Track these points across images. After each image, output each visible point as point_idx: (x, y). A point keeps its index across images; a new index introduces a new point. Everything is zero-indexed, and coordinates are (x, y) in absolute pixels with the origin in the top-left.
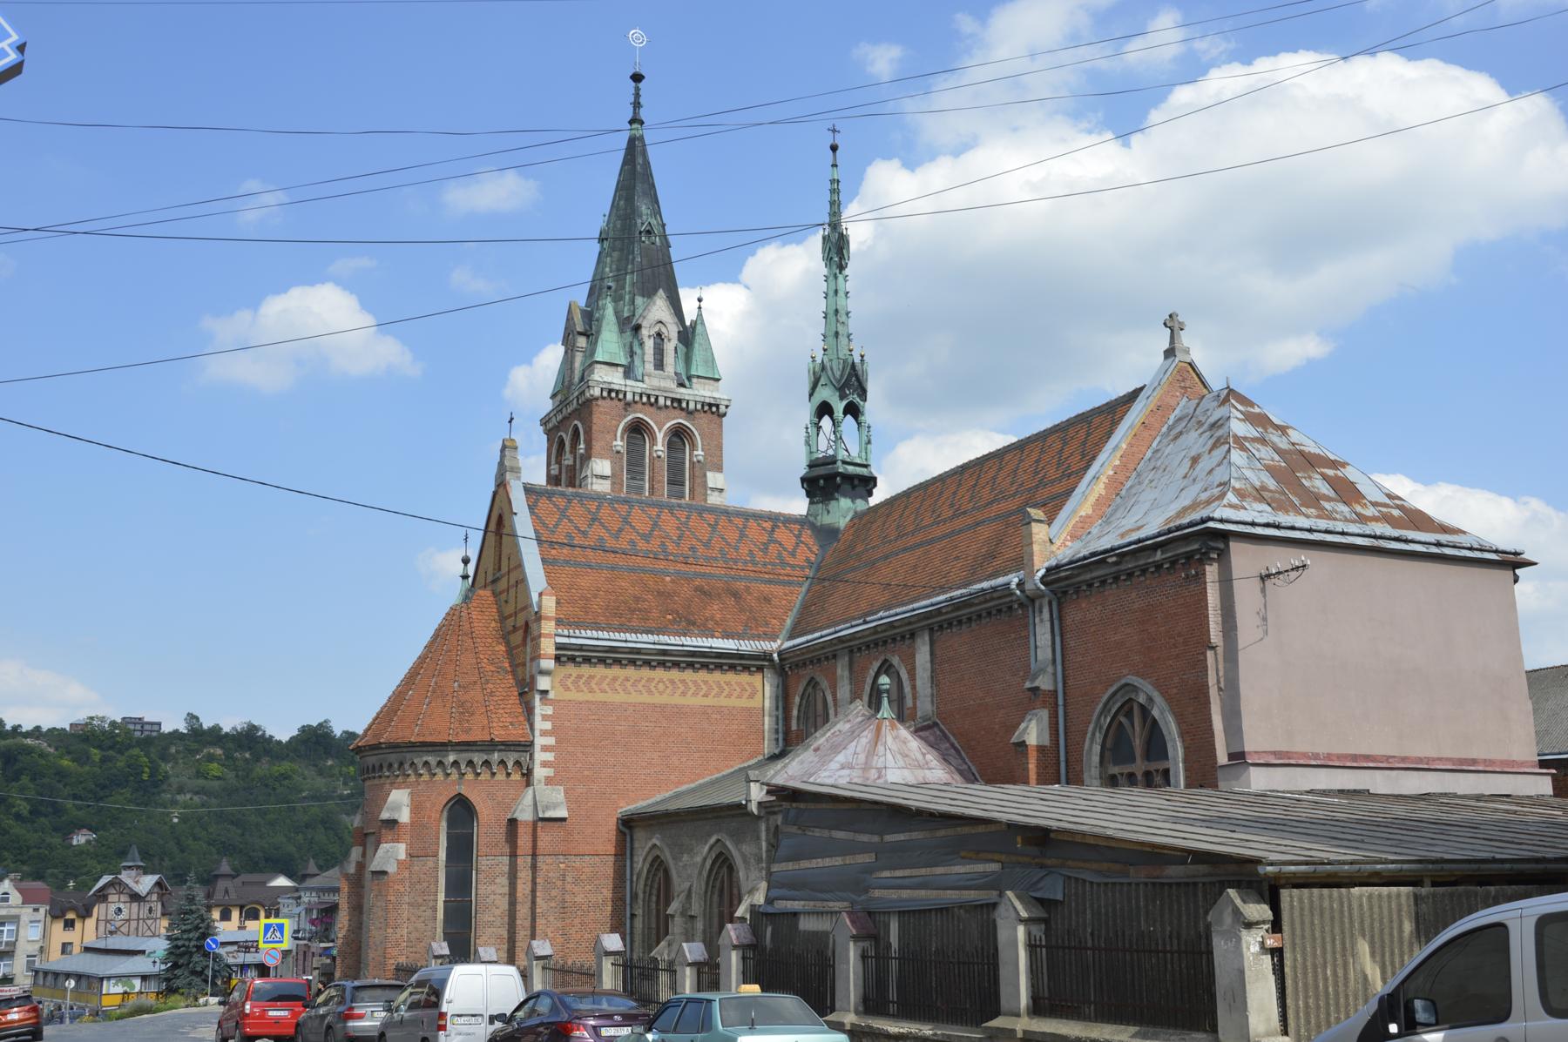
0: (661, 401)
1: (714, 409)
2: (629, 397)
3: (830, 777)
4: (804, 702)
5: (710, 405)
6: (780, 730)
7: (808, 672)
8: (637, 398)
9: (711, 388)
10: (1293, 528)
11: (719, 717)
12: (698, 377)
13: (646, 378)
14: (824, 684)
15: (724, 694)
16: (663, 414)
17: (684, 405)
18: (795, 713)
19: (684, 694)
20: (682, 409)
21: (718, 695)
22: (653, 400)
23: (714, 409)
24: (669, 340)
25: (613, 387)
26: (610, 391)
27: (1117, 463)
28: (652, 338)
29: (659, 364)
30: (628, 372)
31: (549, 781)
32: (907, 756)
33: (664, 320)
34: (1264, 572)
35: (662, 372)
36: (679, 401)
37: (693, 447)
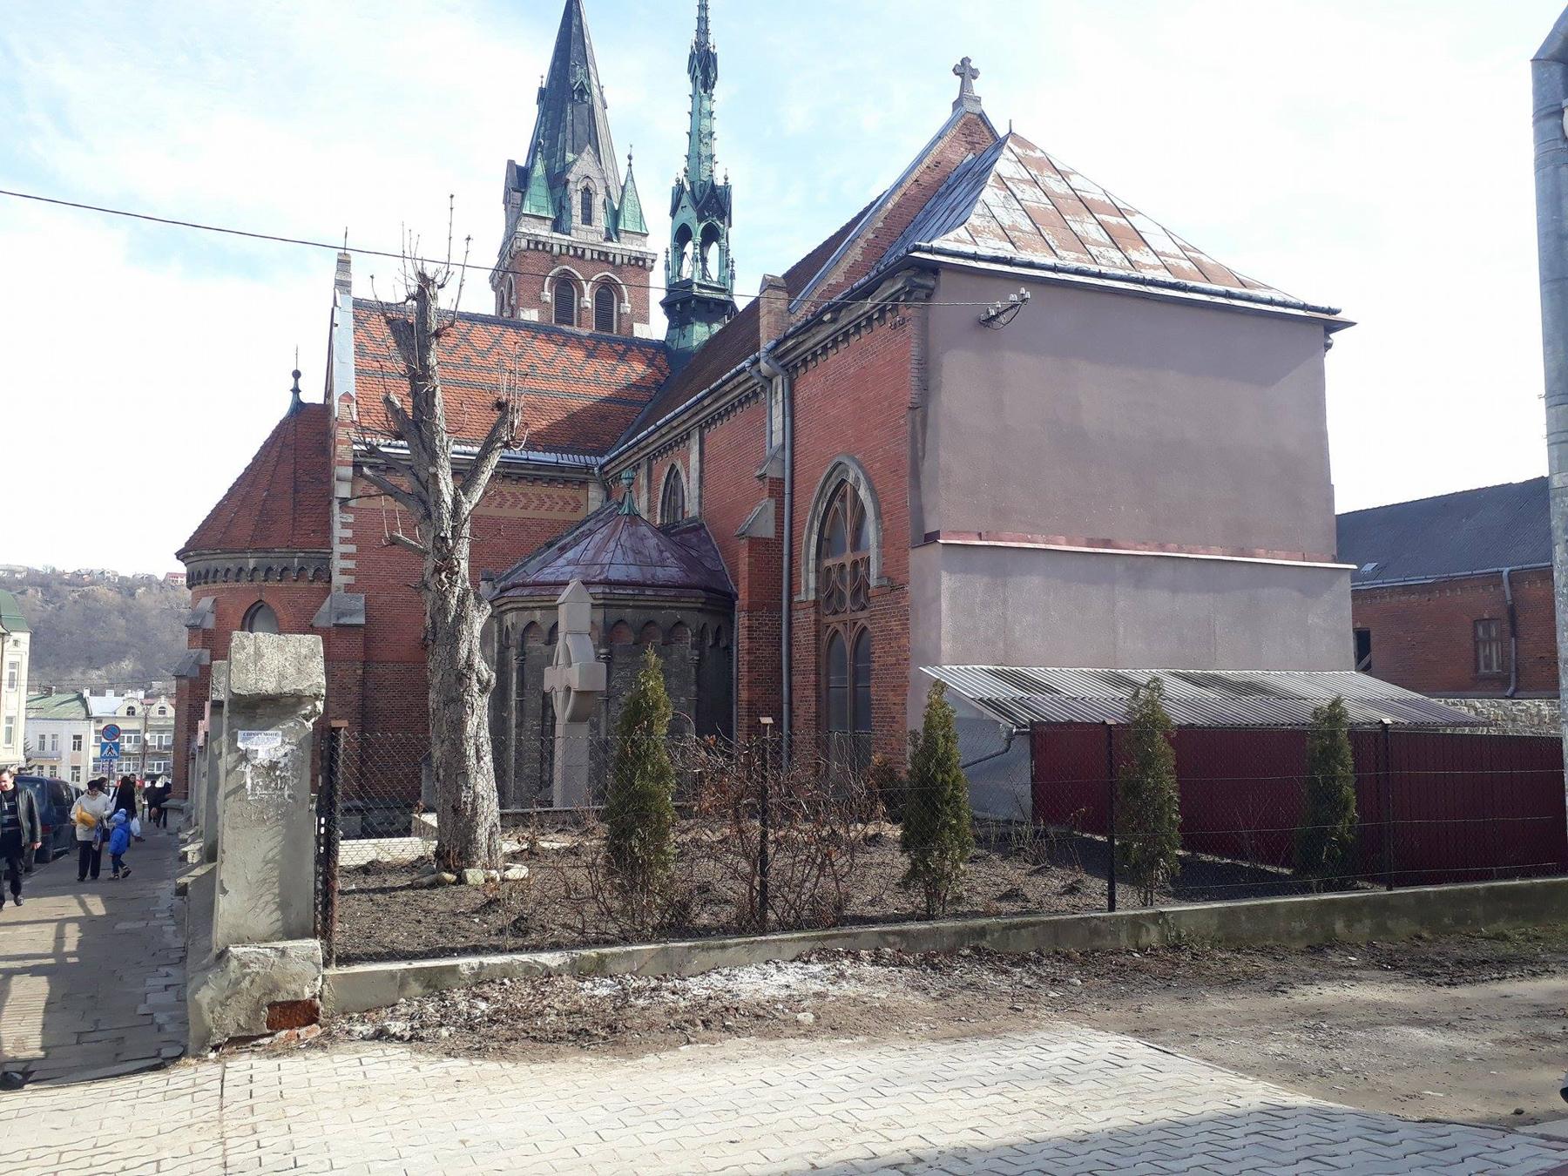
1: (641, 263)
2: (556, 249)
3: (552, 573)
5: (637, 259)
8: (564, 251)
9: (639, 243)
10: (1031, 265)
11: (539, 529)
12: (626, 232)
15: (545, 507)
16: (590, 267)
17: (611, 259)
19: (500, 506)
20: (609, 263)
21: (513, 506)
22: (580, 252)
23: (641, 263)
25: (540, 238)
26: (537, 243)
27: (880, 225)
28: (580, 193)
30: (557, 226)
31: (348, 588)
32: (640, 553)
33: (591, 175)
34: (983, 316)
35: (588, 227)
36: (607, 254)
37: (621, 300)
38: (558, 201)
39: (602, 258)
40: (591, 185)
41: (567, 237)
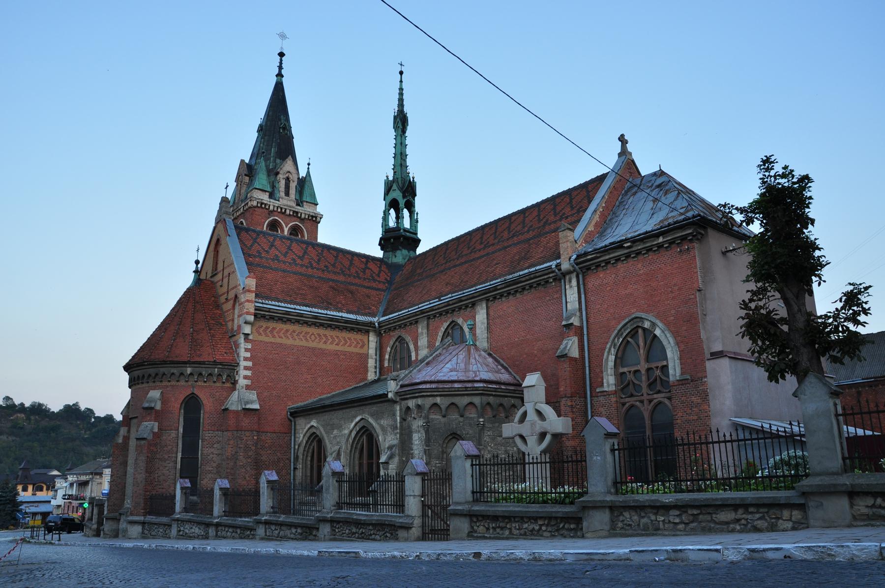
0: (288, 212)
1: (314, 219)
2: (271, 208)
4: (393, 350)
5: (312, 217)
6: (378, 366)
7: (397, 333)
8: (275, 209)
12: (307, 202)
13: (280, 199)
14: (408, 339)
16: (288, 219)
17: (299, 215)
18: (387, 357)
20: (298, 217)
22: (283, 211)
23: (314, 219)
24: (293, 181)
29: (287, 194)
33: (291, 171)
36: (297, 213)
38: (271, 183)
39: (295, 215)
40: (290, 176)
41: (277, 202)
